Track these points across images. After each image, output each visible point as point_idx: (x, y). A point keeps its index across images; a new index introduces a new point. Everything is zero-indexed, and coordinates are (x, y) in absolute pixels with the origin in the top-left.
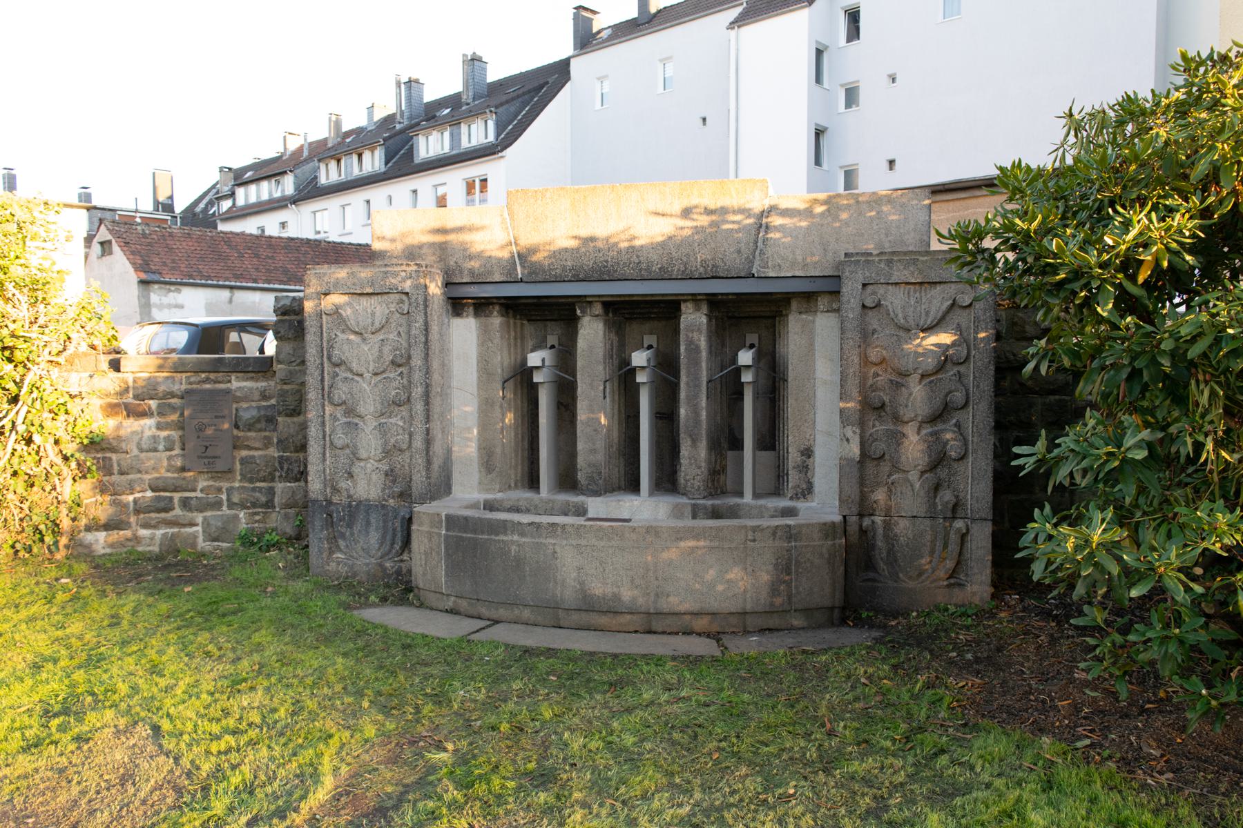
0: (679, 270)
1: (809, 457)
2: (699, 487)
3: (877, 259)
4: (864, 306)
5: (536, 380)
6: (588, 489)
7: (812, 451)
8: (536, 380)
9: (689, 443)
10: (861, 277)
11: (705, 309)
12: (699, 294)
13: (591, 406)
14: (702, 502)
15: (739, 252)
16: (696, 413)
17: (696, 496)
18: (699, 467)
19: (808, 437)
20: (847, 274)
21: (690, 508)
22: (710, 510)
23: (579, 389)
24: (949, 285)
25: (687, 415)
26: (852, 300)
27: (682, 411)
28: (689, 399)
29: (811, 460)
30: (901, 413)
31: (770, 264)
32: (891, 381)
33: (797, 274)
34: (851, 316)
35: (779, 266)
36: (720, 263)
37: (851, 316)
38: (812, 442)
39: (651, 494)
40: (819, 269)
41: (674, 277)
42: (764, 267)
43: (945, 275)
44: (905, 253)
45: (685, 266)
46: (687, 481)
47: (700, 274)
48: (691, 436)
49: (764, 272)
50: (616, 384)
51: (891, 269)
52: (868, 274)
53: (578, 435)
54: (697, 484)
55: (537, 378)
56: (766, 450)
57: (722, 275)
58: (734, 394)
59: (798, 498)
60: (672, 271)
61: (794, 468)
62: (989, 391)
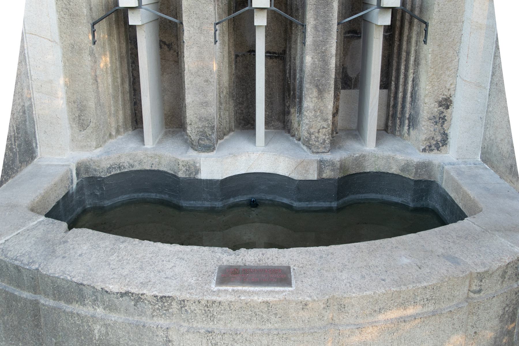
1: (448, 107)
2: (324, 141)
5: (131, 22)
6: (200, 145)
7: (451, 102)
8: (131, 22)
9: (315, 93)
13: (200, 53)
14: (328, 157)
16: (325, 61)
17: (319, 150)
18: (326, 120)
19: (448, 86)
21: (315, 165)
22: (338, 166)
23: (186, 33)
25: (314, 63)
27: (308, 59)
28: (317, 45)
29: (449, 110)
38: (452, 93)
39: (267, 143)
46: (310, 134)
48: (317, 86)
50: (225, 28)
53: (186, 86)
54: (321, 137)
55: (133, 20)
58: (349, 32)
59: (432, 150)
61: (430, 119)
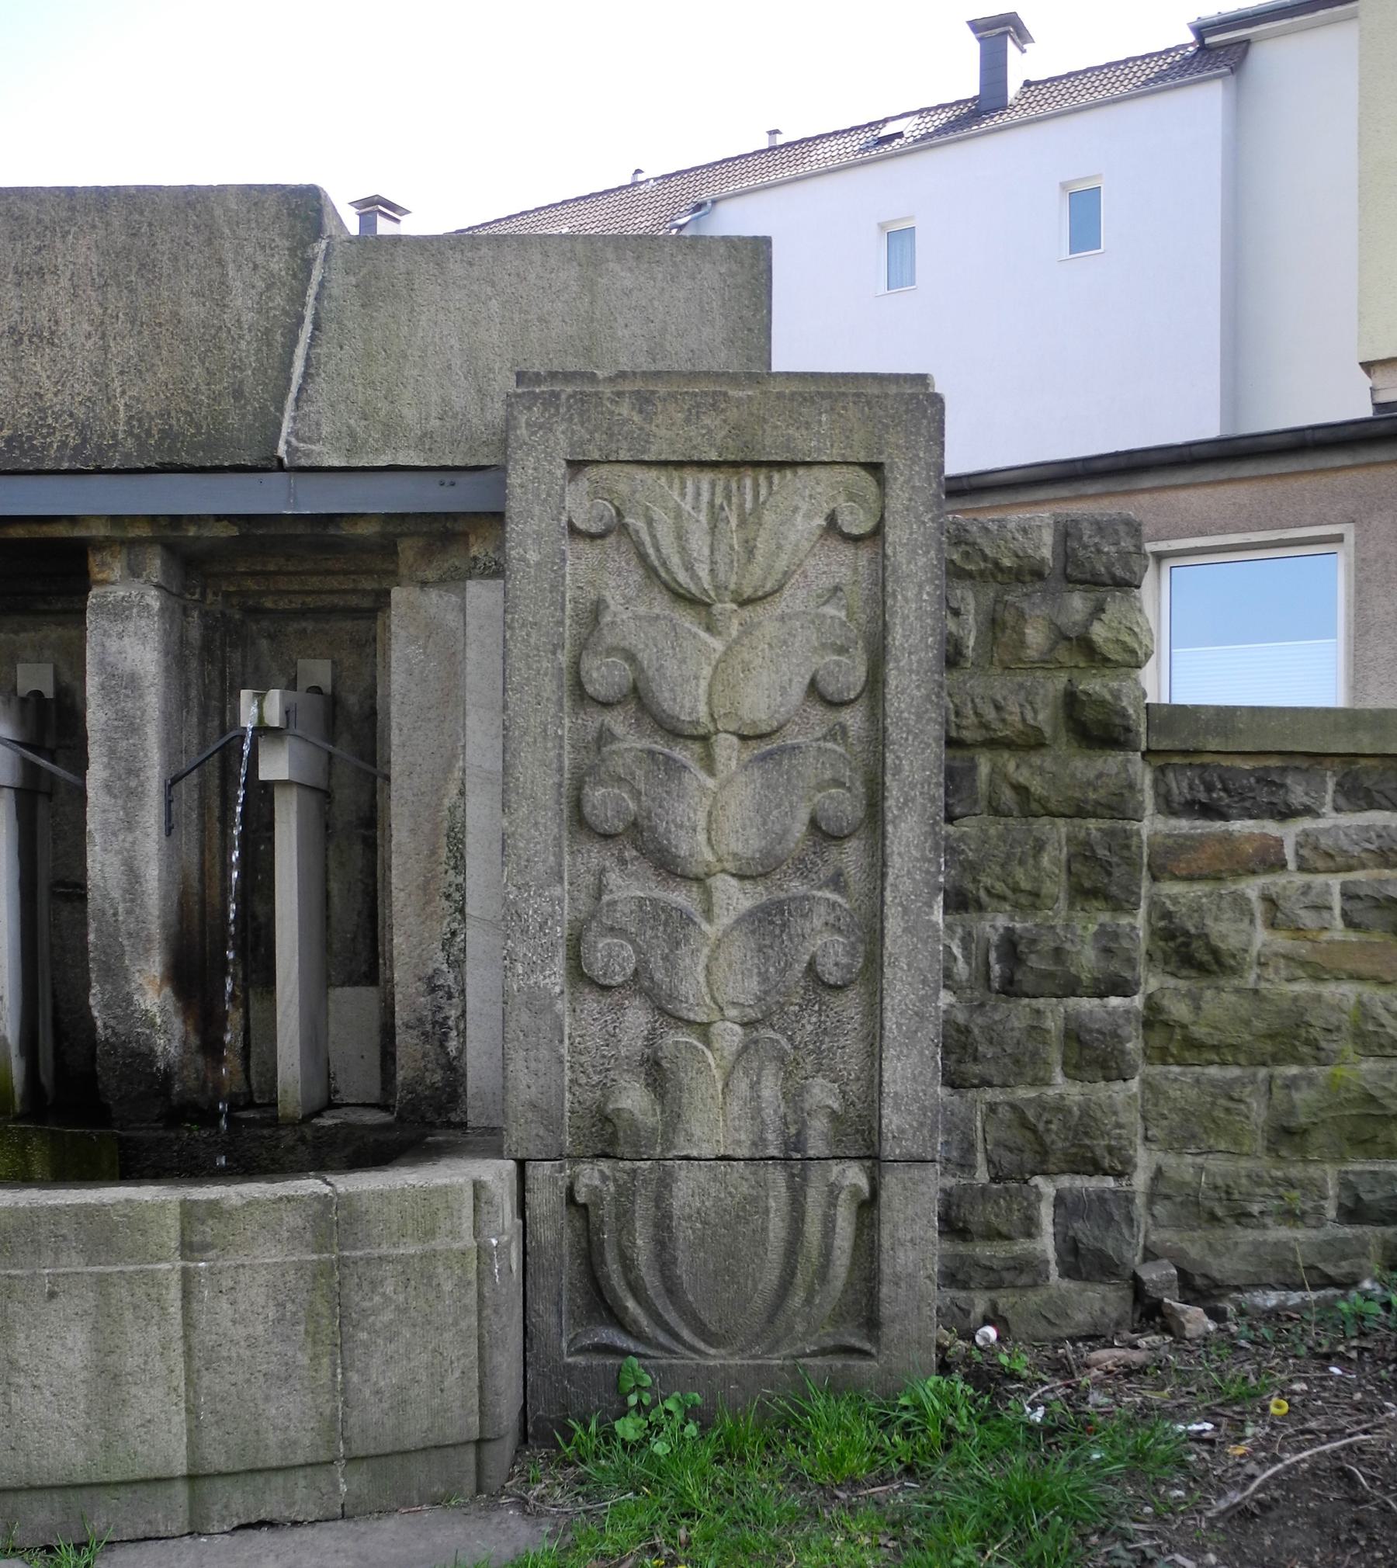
0: (64, 444)
3: (607, 390)
4: (574, 531)
10: (563, 443)
11: (155, 564)
12: (134, 519)
15: (238, 394)
20: (523, 432)
24: (816, 471)
26: (537, 510)
30: (683, 850)
31: (325, 430)
32: (651, 753)
33: (401, 461)
34: (533, 557)
35: (352, 435)
36: (178, 422)
37: (533, 557)
40: (463, 447)
41: (48, 465)
42: (309, 440)
43: (806, 445)
44: (693, 376)
45: (80, 433)
47: (127, 456)
49: (308, 454)
51: (649, 419)
52: (582, 433)
56: (356, 984)
57: (185, 459)
60: (46, 447)
62: (927, 781)
